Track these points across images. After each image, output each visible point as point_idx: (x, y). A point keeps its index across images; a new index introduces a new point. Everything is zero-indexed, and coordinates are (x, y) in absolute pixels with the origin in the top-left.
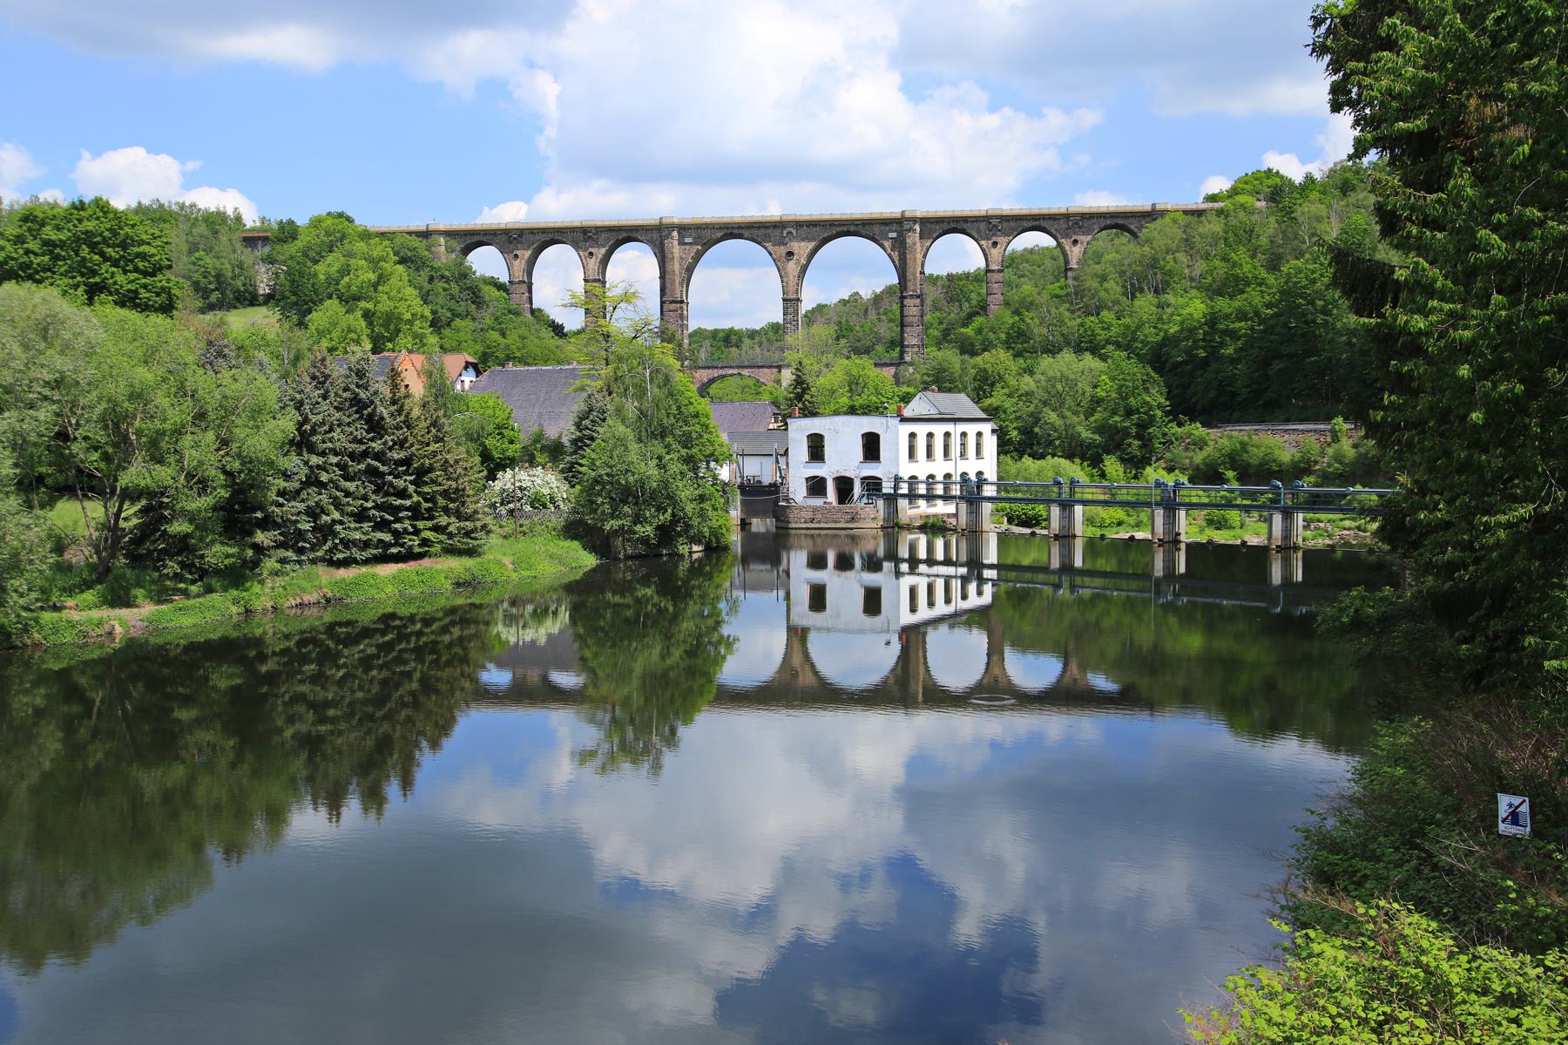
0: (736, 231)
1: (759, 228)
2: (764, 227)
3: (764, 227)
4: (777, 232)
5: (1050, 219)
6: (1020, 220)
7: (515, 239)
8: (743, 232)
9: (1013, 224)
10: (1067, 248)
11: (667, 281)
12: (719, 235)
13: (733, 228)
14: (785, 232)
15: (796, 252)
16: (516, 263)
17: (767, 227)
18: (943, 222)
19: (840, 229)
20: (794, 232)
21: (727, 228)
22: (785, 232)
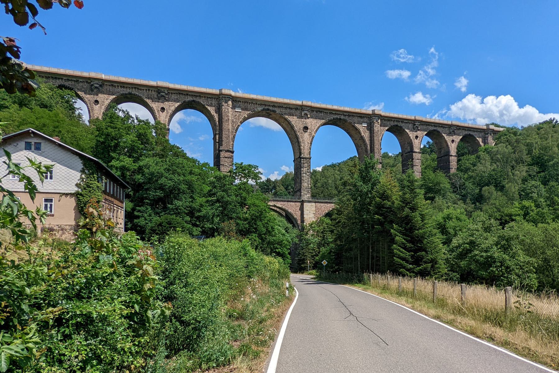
0: (271, 108)
1: (286, 108)
2: (289, 108)
3: (289, 108)
4: (298, 112)
5: (442, 127)
6: (428, 125)
7: (96, 88)
8: (276, 109)
9: (425, 127)
10: (449, 144)
11: (224, 136)
12: (260, 109)
13: (269, 105)
14: (303, 113)
15: (309, 127)
16: (96, 107)
17: (291, 109)
18: (391, 120)
19: (335, 117)
20: (308, 114)
21: (266, 105)
22: (303, 113)
